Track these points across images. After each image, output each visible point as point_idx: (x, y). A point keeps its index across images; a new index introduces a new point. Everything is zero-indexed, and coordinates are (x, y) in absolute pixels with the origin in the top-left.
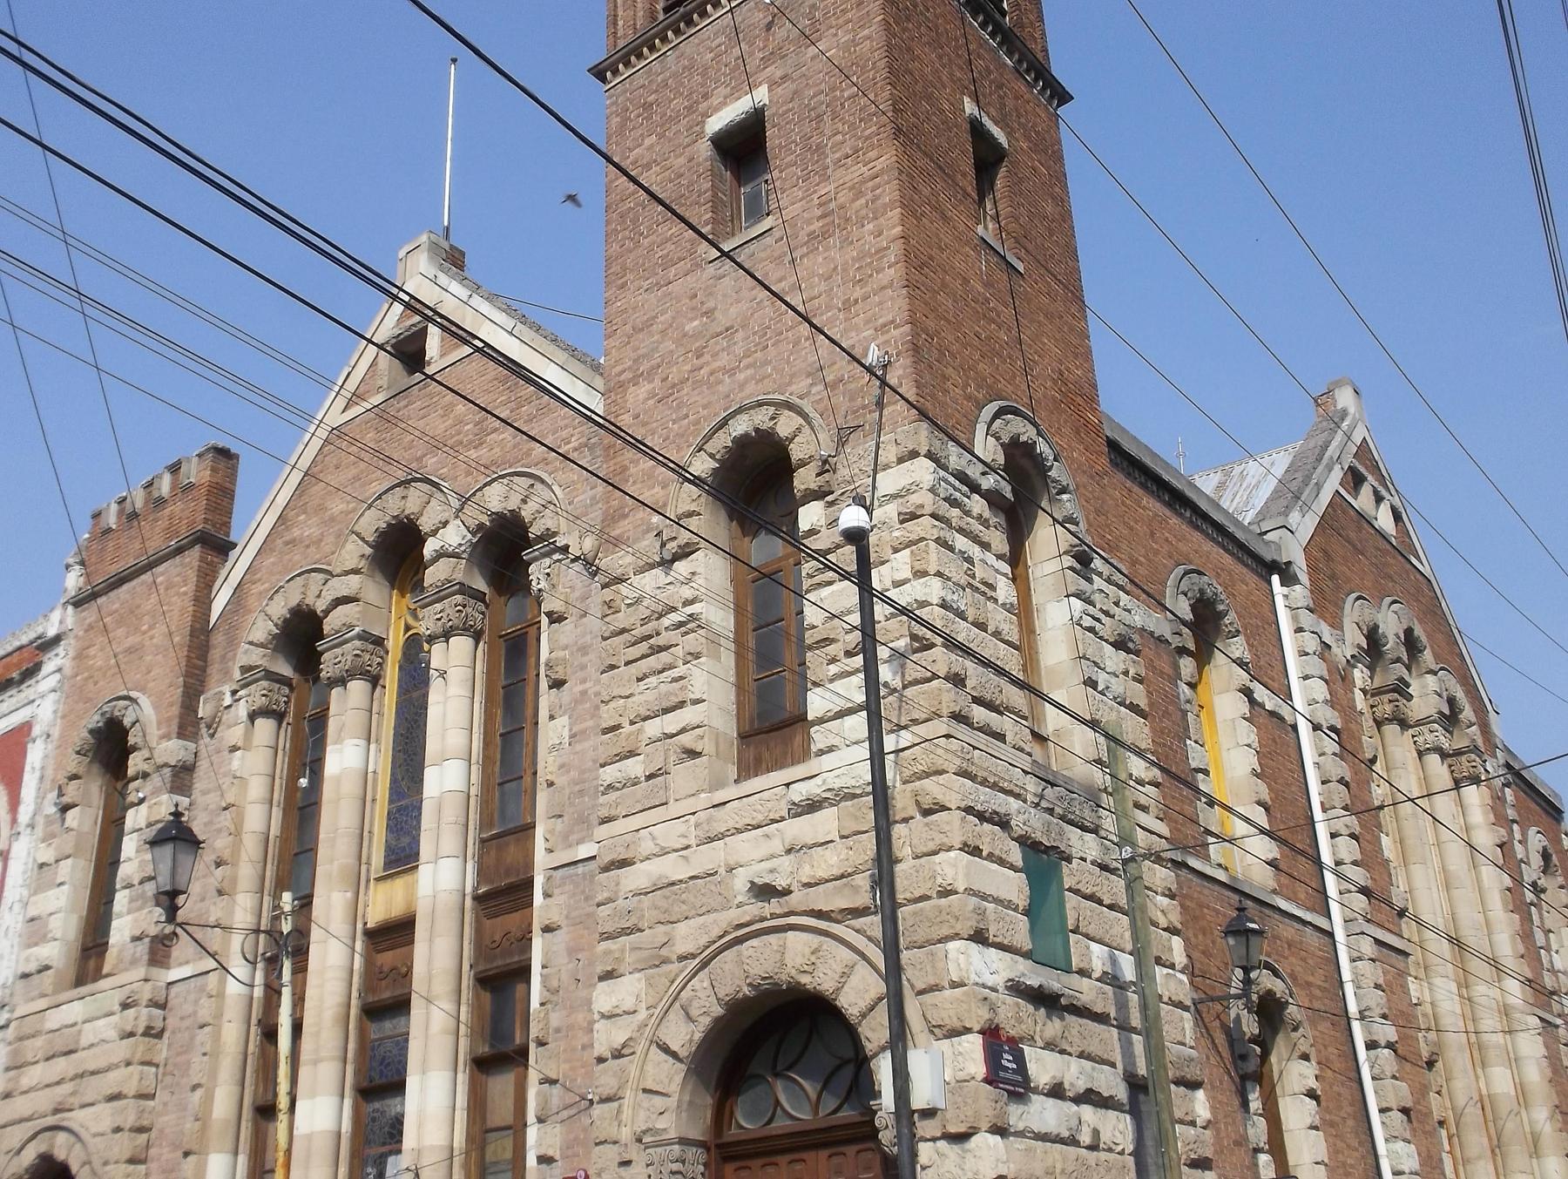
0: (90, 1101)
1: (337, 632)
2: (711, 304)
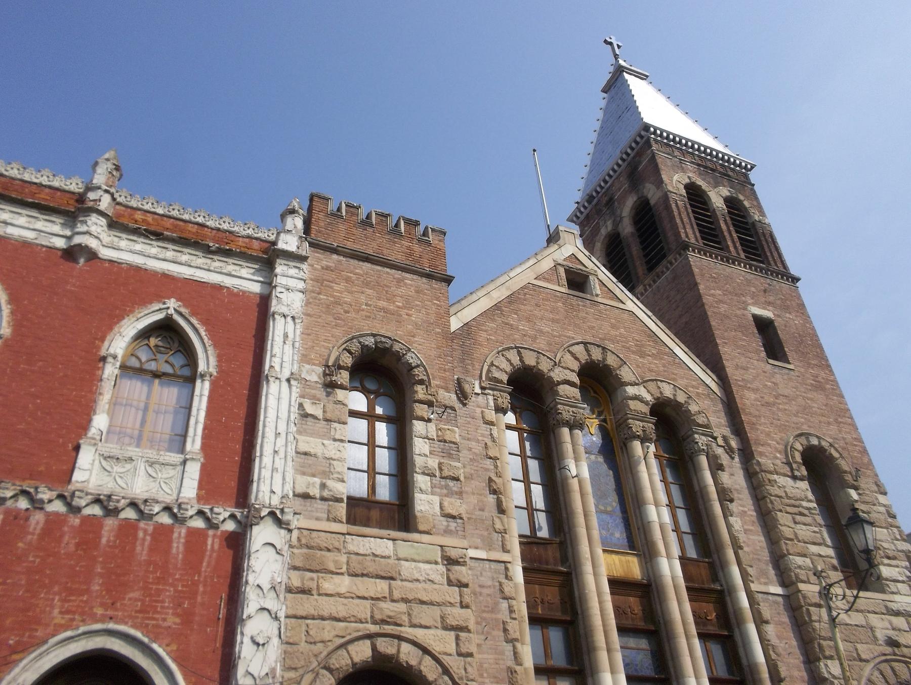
0: (428, 625)
1: (568, 398)
2: (773, 380)
